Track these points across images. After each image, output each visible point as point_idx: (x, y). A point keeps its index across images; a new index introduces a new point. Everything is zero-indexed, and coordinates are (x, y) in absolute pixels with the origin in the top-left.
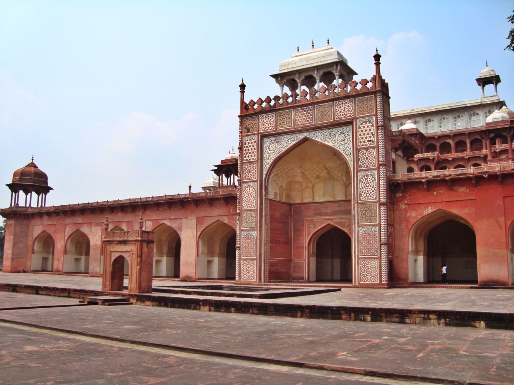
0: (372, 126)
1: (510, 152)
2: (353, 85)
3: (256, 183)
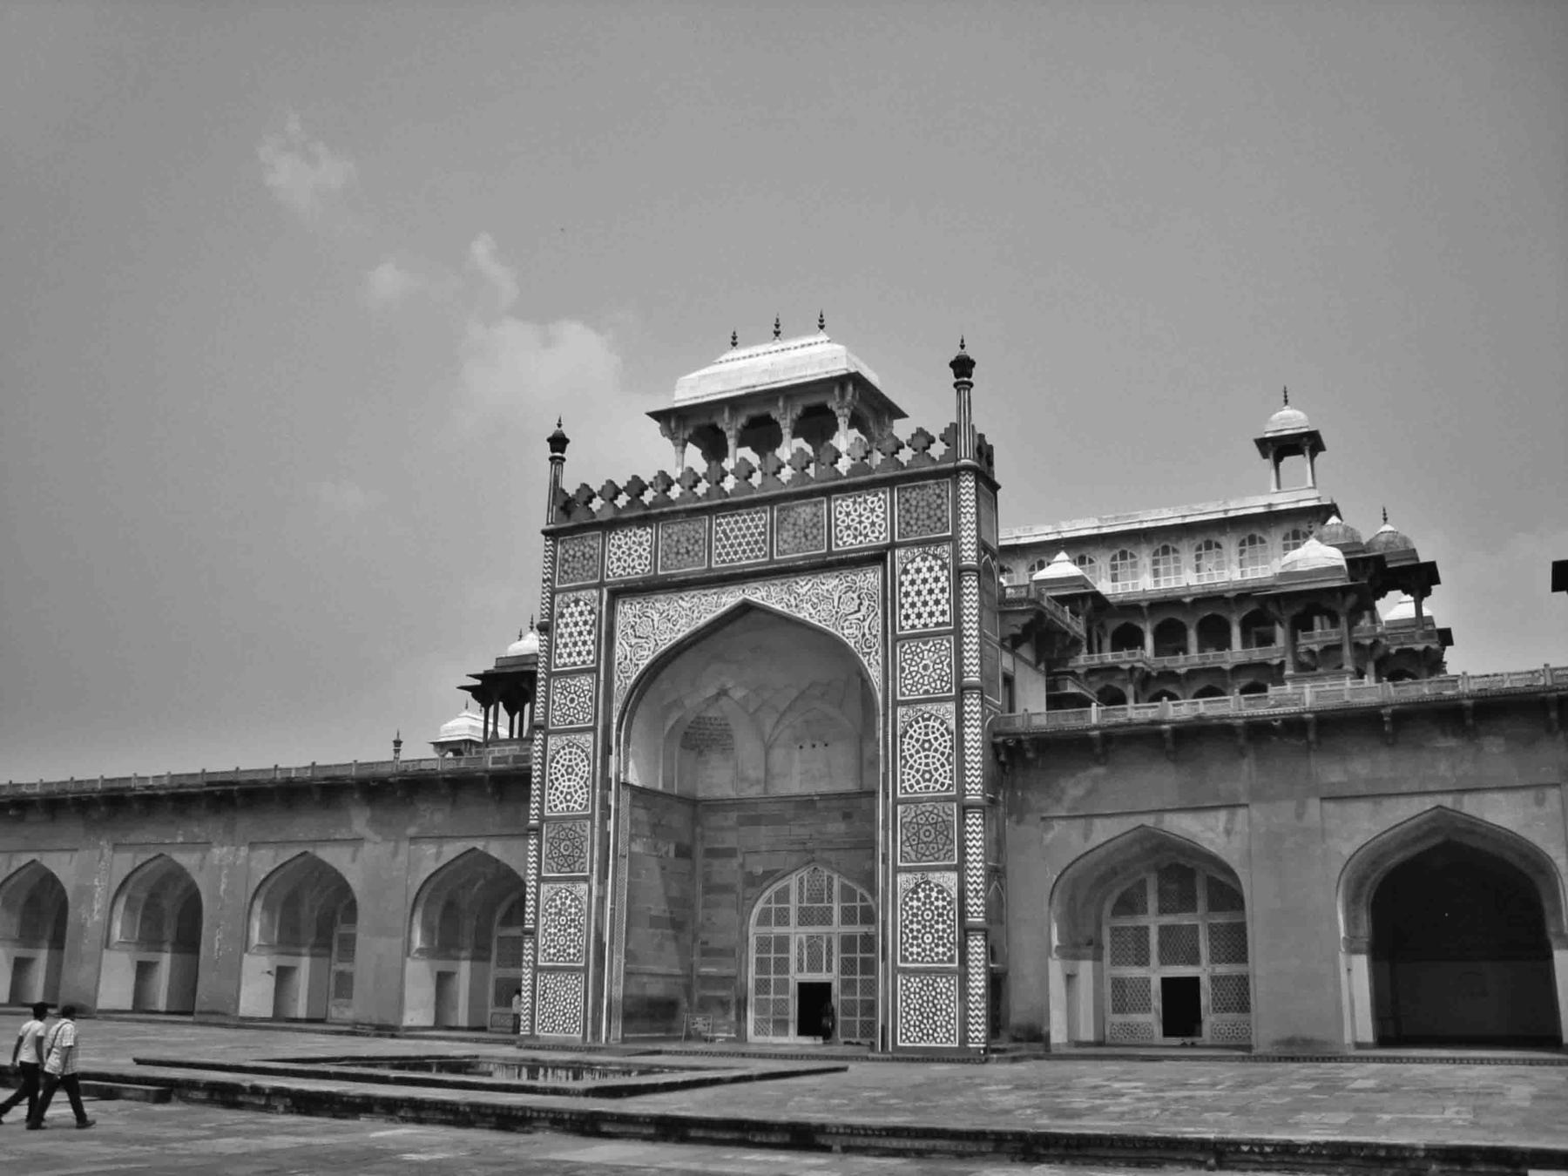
0: (942, 568)
1: (1347, 651)
2: (889, 445)
3: (590, 737)
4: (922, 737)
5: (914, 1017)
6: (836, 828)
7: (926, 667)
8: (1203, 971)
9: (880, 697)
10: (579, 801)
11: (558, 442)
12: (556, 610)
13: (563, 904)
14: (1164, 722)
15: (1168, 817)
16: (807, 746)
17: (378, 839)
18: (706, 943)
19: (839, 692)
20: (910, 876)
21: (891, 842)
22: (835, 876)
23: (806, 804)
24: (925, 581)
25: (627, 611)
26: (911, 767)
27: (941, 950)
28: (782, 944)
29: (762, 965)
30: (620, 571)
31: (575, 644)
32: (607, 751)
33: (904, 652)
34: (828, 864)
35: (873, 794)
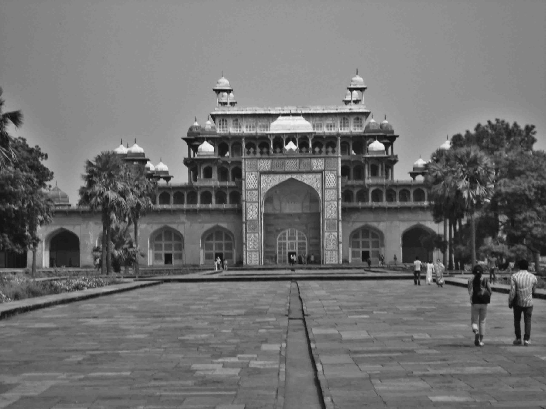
6: (297, 220)
8: (370, 250)
10: (255, 217)
19: (313, 198)
23: (290, 215)
25: (264, 177)
28: (285, 244)
29: (280, 249)
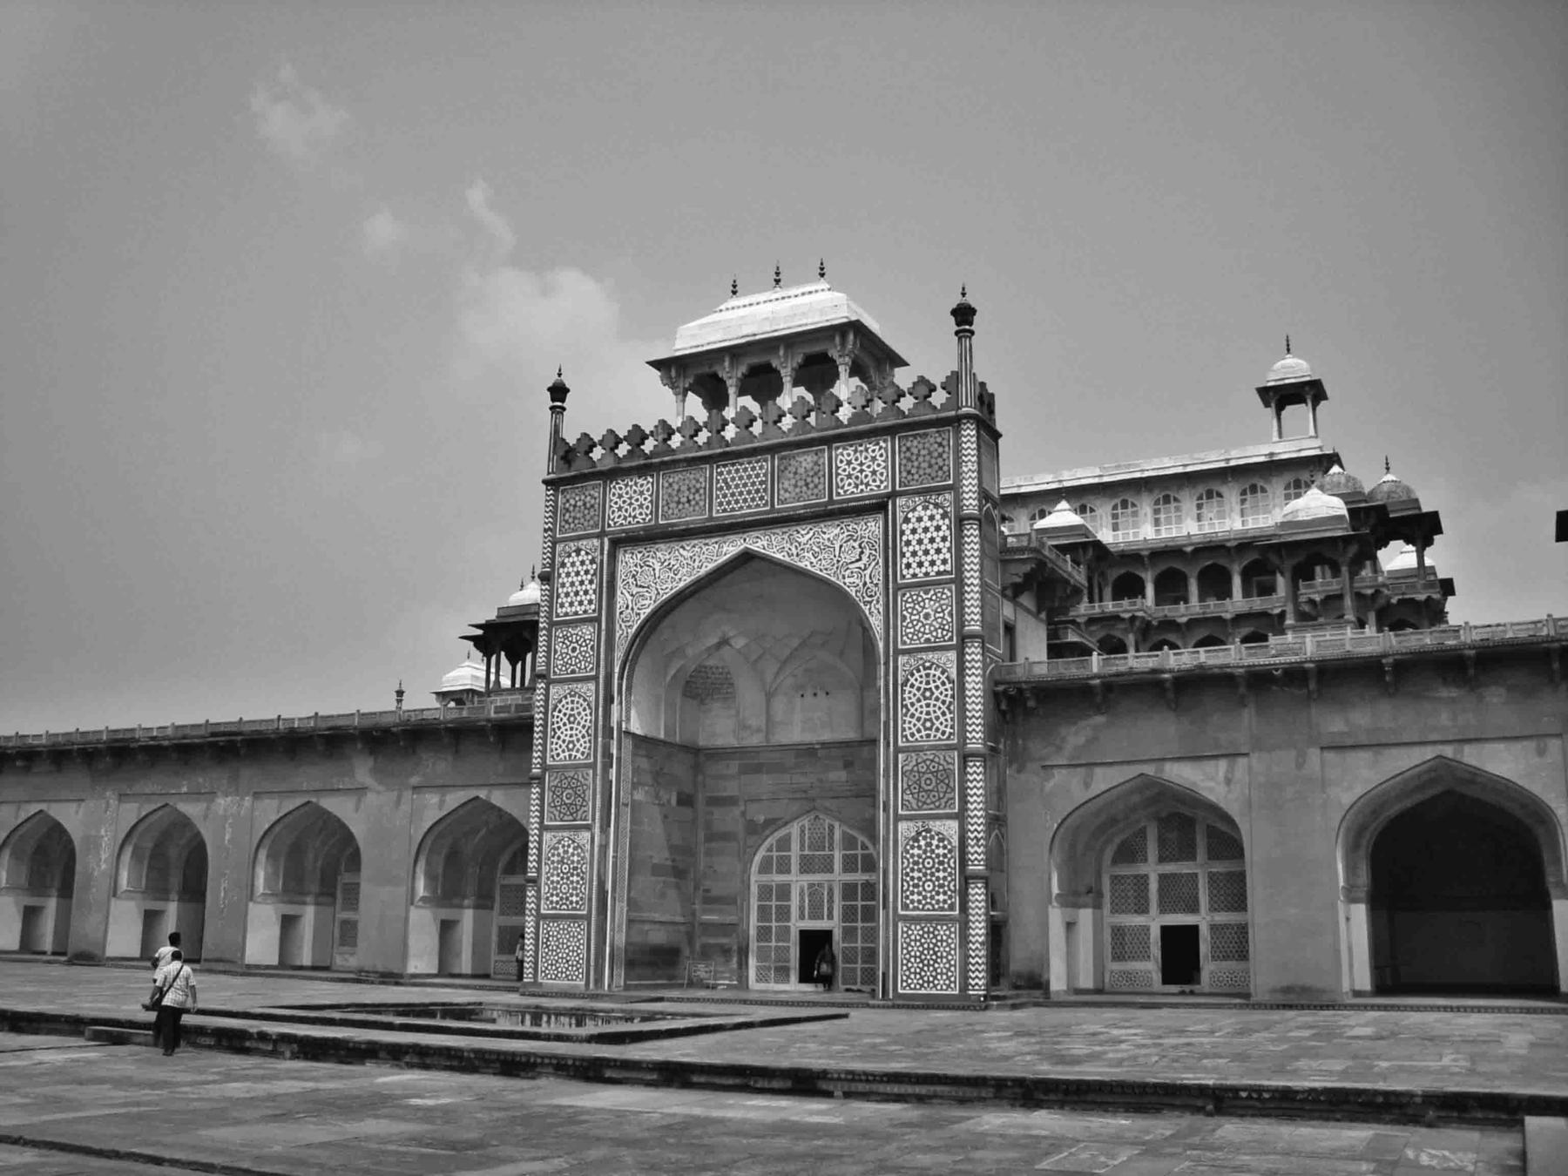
0: (944, 516)
1: (1348, 602)
2: (890, 393)
3: (592, 686)
4: (923, 686)
5: (915, 965)
6: (838, 776)
7: (927, 616)
8: (1203, 920)
9: (881, 645)
11: (559, 392)
12: (558, 560)
13: (566, 852)
14: (1163, 671)
15: (1168, 766)
16: (809, 694)
17: (381, 788)
18: (707, 891)
20: (911, 824)
21: (892, 790)
22: (837, 825)
23: (808, 752)
24: (926, 530)
25: (628, 560)
26: (913, 716)
27: (941, 897)
28: (784, 892)
29: (764, 912)
30: (620, 521)
31: (577, 593)
32: (609, 700)
33: (906, 601)
34: (827, 811)
35: (874, 742)
